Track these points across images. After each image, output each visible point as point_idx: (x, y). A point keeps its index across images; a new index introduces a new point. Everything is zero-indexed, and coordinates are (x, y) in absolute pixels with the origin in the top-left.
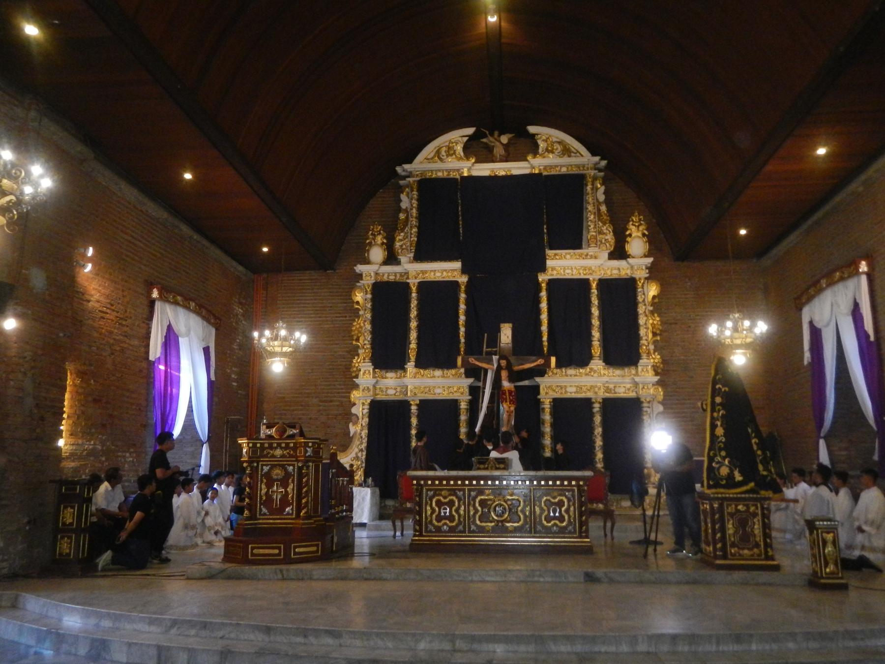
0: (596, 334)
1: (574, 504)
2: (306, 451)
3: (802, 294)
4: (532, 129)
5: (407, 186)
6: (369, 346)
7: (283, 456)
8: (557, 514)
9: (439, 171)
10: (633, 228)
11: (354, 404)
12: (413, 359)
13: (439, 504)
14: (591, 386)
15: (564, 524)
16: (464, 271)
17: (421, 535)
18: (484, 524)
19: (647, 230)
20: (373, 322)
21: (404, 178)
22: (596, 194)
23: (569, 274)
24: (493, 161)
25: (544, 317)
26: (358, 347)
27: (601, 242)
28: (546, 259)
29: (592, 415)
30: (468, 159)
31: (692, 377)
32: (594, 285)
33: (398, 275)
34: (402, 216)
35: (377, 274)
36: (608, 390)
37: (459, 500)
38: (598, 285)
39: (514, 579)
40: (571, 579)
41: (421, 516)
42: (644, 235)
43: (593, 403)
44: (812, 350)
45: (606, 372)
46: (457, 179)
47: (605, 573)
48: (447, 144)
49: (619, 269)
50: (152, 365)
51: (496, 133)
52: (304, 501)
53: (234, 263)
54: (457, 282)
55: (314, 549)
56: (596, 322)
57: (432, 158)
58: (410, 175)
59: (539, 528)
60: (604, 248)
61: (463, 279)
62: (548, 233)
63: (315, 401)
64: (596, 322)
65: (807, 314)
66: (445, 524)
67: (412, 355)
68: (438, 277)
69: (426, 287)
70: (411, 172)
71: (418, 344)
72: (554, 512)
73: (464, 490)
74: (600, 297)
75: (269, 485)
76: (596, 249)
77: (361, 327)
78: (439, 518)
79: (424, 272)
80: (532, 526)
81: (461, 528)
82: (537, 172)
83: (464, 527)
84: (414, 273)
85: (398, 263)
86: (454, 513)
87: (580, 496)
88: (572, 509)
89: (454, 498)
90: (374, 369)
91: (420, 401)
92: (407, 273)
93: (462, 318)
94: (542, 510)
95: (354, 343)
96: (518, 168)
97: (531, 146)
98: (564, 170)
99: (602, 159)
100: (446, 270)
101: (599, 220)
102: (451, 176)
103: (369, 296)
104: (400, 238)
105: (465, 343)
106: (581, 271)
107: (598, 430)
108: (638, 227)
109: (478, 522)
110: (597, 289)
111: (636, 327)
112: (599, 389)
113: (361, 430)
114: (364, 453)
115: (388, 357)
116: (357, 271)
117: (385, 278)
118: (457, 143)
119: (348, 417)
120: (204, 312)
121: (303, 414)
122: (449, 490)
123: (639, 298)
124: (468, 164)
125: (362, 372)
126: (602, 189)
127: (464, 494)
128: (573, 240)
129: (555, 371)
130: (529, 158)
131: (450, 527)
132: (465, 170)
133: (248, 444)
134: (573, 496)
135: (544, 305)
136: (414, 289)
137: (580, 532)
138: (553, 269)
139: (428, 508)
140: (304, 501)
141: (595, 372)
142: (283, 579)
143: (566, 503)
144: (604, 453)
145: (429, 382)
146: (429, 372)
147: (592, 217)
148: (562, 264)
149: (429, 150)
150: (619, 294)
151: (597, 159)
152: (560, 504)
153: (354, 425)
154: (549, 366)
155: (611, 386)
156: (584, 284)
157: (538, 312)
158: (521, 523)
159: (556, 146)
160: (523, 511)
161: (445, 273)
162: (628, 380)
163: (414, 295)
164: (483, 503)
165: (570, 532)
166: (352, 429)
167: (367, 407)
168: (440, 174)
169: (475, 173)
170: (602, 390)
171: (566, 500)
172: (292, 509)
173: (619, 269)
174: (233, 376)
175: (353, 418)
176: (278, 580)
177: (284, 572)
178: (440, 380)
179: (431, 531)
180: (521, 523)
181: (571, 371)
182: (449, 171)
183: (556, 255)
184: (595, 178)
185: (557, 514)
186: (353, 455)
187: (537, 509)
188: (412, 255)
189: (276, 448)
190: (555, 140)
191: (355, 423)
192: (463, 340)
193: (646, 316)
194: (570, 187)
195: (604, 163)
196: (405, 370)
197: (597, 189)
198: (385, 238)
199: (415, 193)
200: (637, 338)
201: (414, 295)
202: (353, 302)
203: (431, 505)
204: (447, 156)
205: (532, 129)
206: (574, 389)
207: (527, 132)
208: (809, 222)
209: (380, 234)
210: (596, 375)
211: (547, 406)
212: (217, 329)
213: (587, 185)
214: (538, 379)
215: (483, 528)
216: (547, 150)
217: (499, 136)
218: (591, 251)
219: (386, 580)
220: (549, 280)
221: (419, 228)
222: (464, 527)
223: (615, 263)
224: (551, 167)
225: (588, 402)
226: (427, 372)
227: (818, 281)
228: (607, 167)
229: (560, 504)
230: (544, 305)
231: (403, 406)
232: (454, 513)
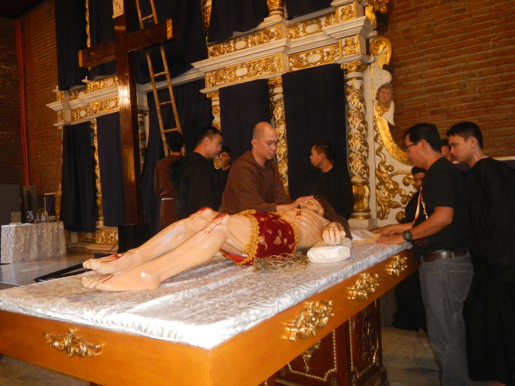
14: (270, 60)
31: (463, 10)
43: (273, 86)
45: (292, 32)
91: (98, 119)
144: (289, 165)
155: (303, 56)
162: (320, 38)
181: (241, 44)
196: (85, 84)
206: (245, 71)
210: (273, 41)
211: (216, 102)
214: (196, 65)
225: (262, 87)
226: (102, 83)
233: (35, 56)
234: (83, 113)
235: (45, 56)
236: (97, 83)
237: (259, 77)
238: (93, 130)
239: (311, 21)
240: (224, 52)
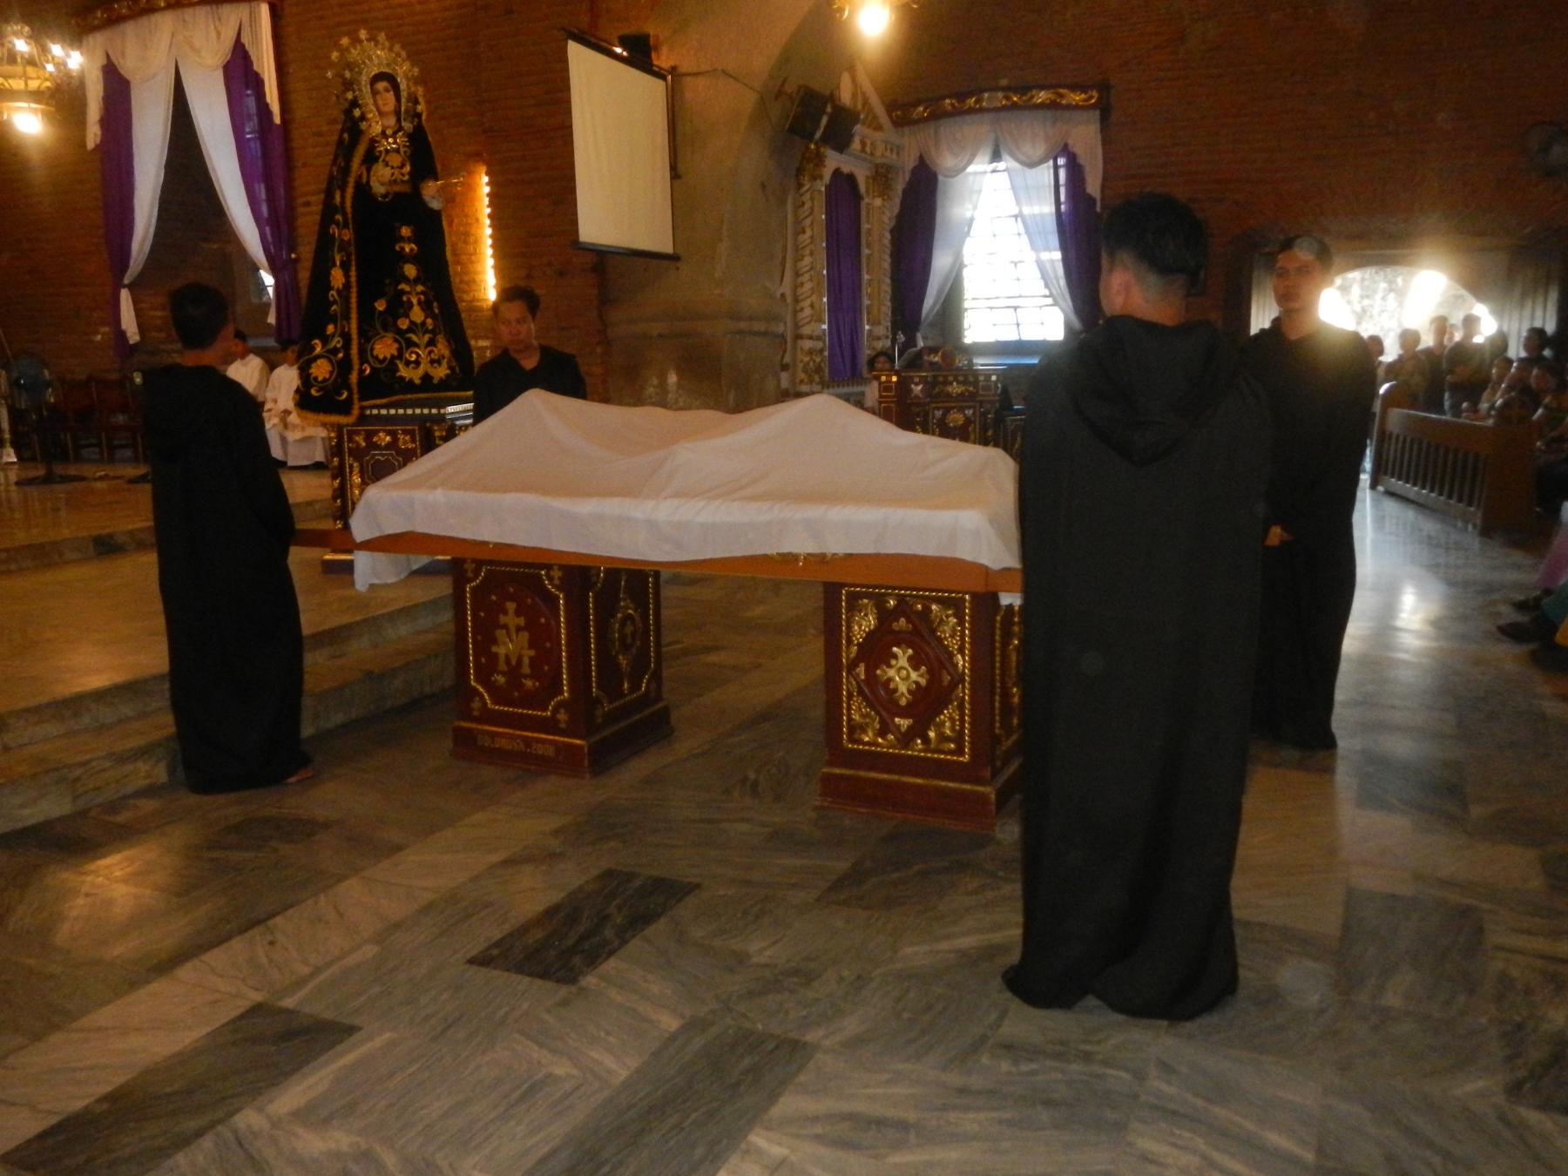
44: (105, 122)
47: (131, 533)
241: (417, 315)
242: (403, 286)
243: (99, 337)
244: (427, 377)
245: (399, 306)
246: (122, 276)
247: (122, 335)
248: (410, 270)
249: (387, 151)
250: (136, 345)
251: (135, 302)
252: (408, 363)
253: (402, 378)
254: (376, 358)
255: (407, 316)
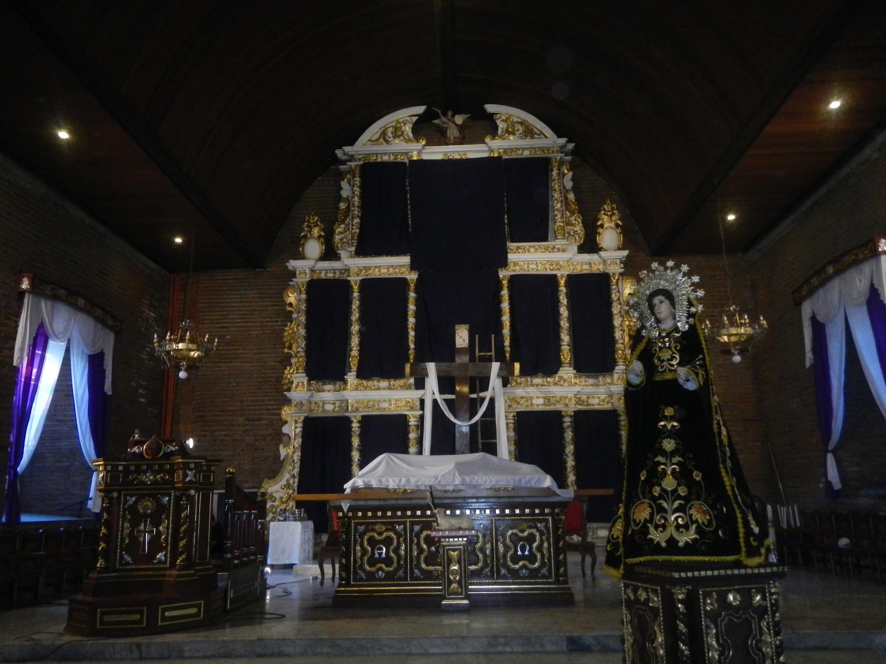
0: (565, 338)
1: (548, 540)
2: (185, 476)
3: (802, 286)
4: (490, 108)
5: (349, 172)
6: (303, 354)
7: (155, 482)
8: (526, 553)
9: (385, 154)
10: (606, 218)
11: (286, 422)
12: (354, 368)
13: (373, 542)
14: (561, 398)
15: (537, 565)
16: (413, 267)
17: (348, 584)
18: (431, 568)
19: (620, 219)
20: (308, 327)
21: (344, 162)
22: (562, 182)
23: (533, 270)
24: (447, 144)
25: (506, 319)
26: (291, 356)
27: (569, 234)
28: (506, 253)
29: (562, 430)
30: (418, 141)
32: (562, 282)
33: (338, 273)
34: (343, 206)
35: (313, 271)
36: (579, 401)
37: (399, 535)
38: (566, 282)
39: (469, 650)
40: (550, 647)
41: (348, 560)
42: (617, 226)
43: (564, 416)
44: (814, 350)
45: (578, 381)
46: (405, 164)
47: (596, 638)
48: (394, 124)
49: (590, 264)
50: (17, 370)
51: (450, 113)
52: (182, 544)
53: (143, 259)
54: (405, 279)
55: (193, 611)
56: (564, 324)
57: (377, 140)
58: (352, 158)
59: (503, 571)
60: (573, 240)
61: (413, 277)
62: (509, 224)
63: (241, 420)
64: (564, 324)
65: (807, 309)
66: (381, 569)
67: (354, 363)
68: (384, 273)
69: (370, 286)
70: (352, 156)
71: (361, 351)
72: (523, 550)
73: (405, 523)
74: (569, 296)
75: (134, 524)
76: (564, 242)
77: (295, 333)
78: (372, 562)
79: (367, 268)
80: (495, 568)
81: (401, 573)
82: (496, 155)
83: (405, 572)
84: (356, 270)
85: (337, 258)
86: (392, 554)
87: (556, 528)
88: (546, 545)
89: (392, 534)
90: (309, 381)
92: (347, 270)
93: (412, 320)
94: (507, 548)
95: (286, 350)
96: (474, 151)
97: (487, 126)
98: (526, 154)
99: (568, 142)
100: (394, 266)
101: (567, 209)
102: (399, 160)
103: (304, 296)
104: (340, 230)
105: (414, 349)
106: (547, 266)
107: (570, 449)
108: (611, 216)
109: (423, 566)
110: (566, 286)
111: (612, 328)
112: (570, 400)
113: (294, 453)
114: (297, 480)
115: (325, 367)
116: (290, 268)
117: (323, 276)
118: (405, 124)
119: (279, 438)
120: (99, 312)
121: (226, 435)
122: (385, 524)
123: (613, 296)
124: (419, 146)
125: (294, 385)
126: (570, 174)
127: (405, 529)
128: (538, 231)
129: (519, 380)
130: (488, 140)
131: (387, 573)
132: (415, 153)
133: (105, 466)
134: (547, 527)
135: (505, 306)
136: (356, 288)
137: (557, 575)
138: (515, 264)
139: (358, 548)
140: (182, 544)
141: (565, 381)
142: (141, 658)
143: (538, 538)
144: (576, 475)
145: (373, 395)
146: (374, 383)
147: (559, 205)
148: (525, 258)
149: (373, 130)
150: (592, 291)
151: (565, 139)
152: (531, 539)
153: (284, 447)
154: (512, 373)
155: (584, 397)
156: (551, 280)
157: (499, 313)
158: (480, 564)
159: (518, 127)
160: (482, 549)
161: (391, 269)
162: (602, 389)
163: (356, 294)
164: (429, 540)
165: (544, 577)
166: (283, 451)
167: (300, 425)
168: (386, 158)
169: (425, 157)
170: (574, 402)
171: (537, 534)
172: (165, 556)
173: (590, 264)
174: (141, 391)
175: (285, 439)
176: (133, 659)
177: (143, 648)
178: (386, 394)
179: (361, 579)
180: (480, 564)
181: (537, 381)
182: (396, 154)
183: (518, 248)
184: (561, 163)
185: (526, 553)
186: (284, 482)
187: (501, 548)
188: (353, 249)
189: (145, 472)
190: (515, 120)
191: (287, 445)
192: (412, 346)
193: (622, 316)
194: (535, 170)
195: (571, 146)
197: (564, 175)
198: (323, 230)
199: (357, 179)
200: (613, 341)
201: (356, 294)
202: (286, 304)
203: (362, 545)
204: (394, 138)
205: (490, 108)
206: (541, 401)
207: (484, 111)
208: (808, 203)
209: (317, 226)
210: (566, 384)
212: (116, 334)
213: (552, 171)
215: (431, 572)
216: (507, 131)
217: (453, 116)
218: (559, 243)
219: (289, 655)
220: (512, 276)
221: (361, 219)
222: (405, 572)
223: (586, 257)
224: (512, 150)
225: (557, 416)
226: (370, 383)
227: (823, 269)
228: (573, 153)
229: (531, 539)
230: (505, 306)
231: (341, 424)
232: (392, 554)
233: (203, 324)
234: (329, 407)
235: (225, 327)
236: (365, 382)
237: (551, 408)
238: (350, 428)
239: (592, 377)
240: (521, 383)
241: (669, 483)
242: (660, 459)
243: (821, 486)
244: (672, 541)
245: (656, 477)
246: (827, 445)
247: (829, 484)
248: (669, 445)
249: (661, 348)
250: (838, 491)
251: (838, 461)
252: (656, 527)
253: (652, 540)
254: (635, 521)
255: (660, 485)
